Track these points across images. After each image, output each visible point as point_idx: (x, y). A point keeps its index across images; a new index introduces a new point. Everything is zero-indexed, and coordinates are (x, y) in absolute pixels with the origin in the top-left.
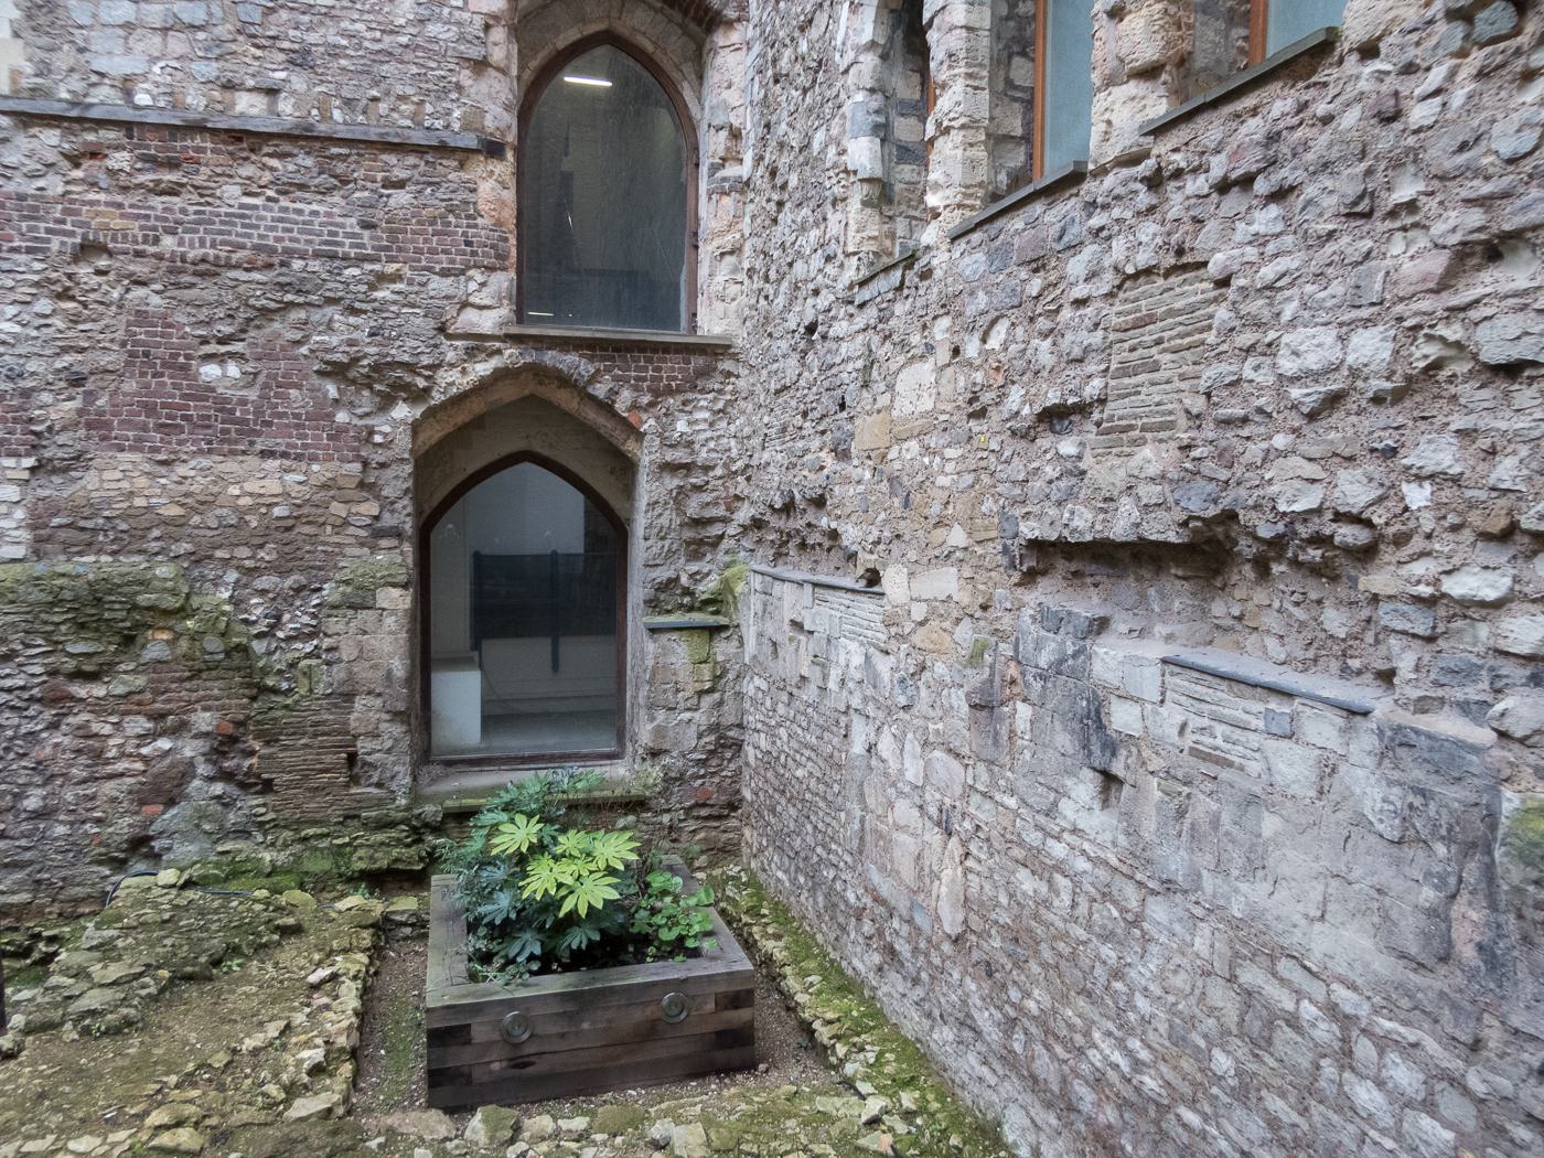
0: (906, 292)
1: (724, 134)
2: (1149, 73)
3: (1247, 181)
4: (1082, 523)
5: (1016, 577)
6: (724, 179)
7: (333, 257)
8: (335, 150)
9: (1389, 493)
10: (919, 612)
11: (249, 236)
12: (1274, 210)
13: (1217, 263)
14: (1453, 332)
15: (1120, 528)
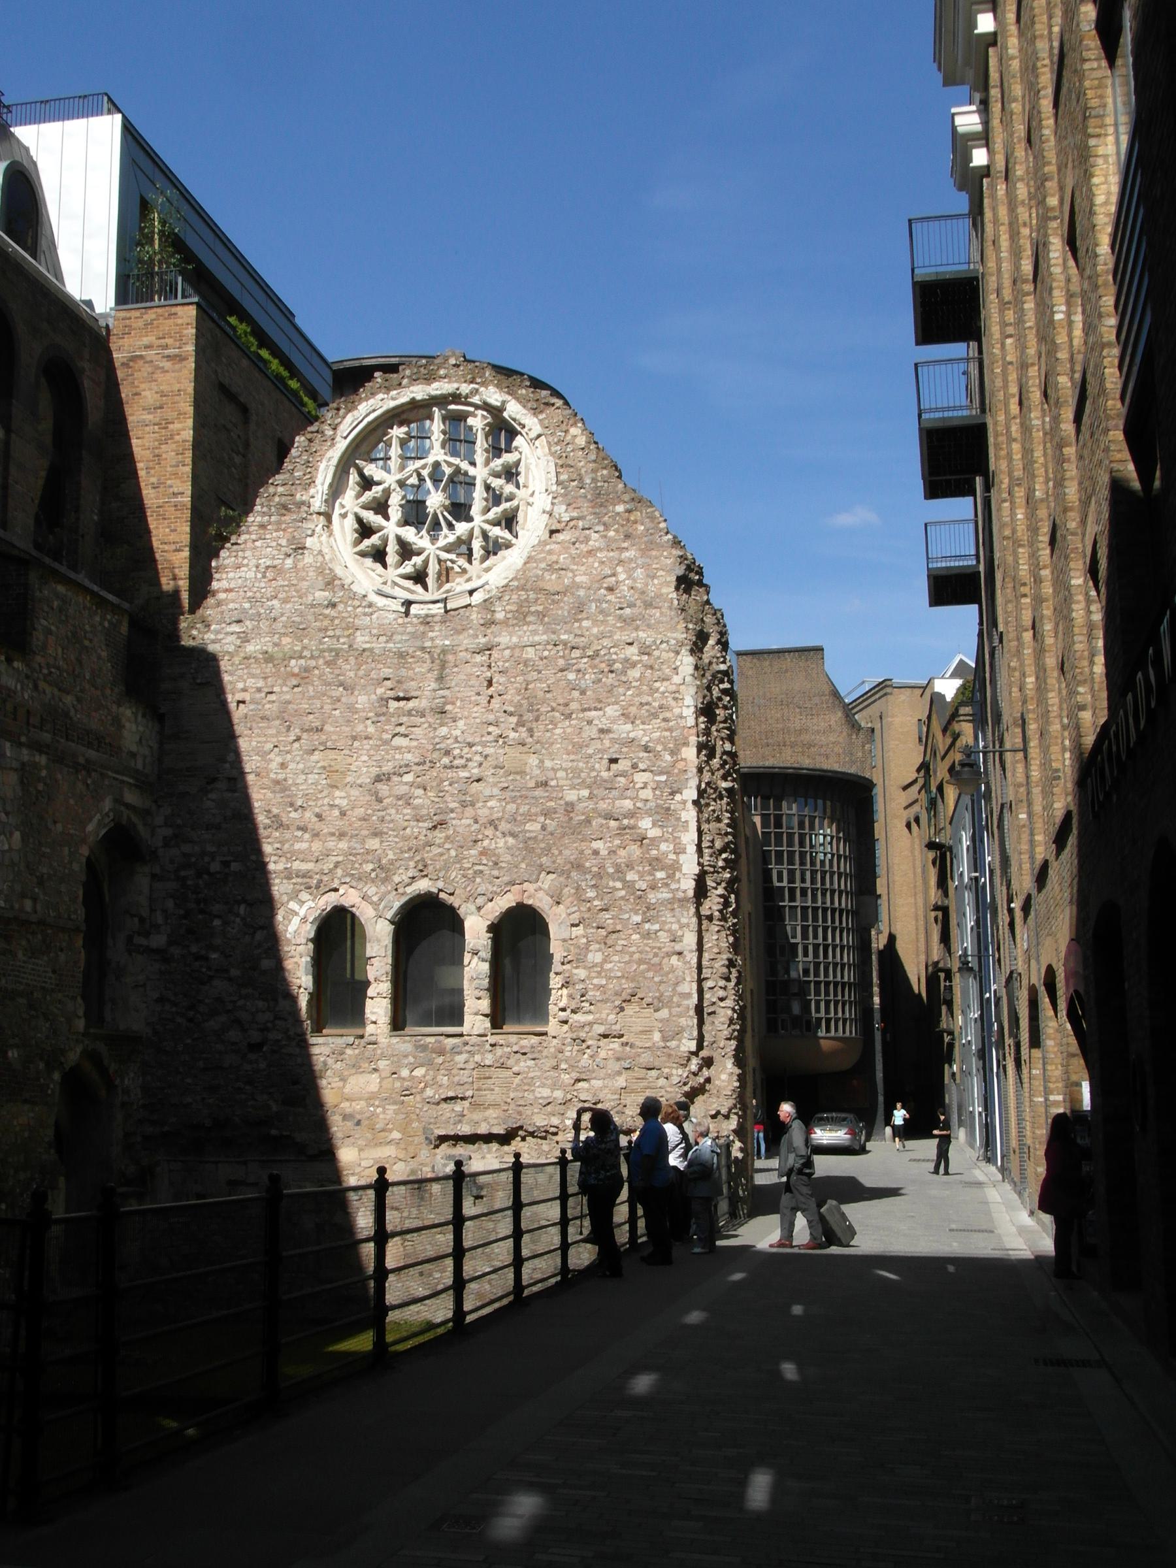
0: (354, 1046)
1: (136, 920)
2: (486, 1016)
3: (524, 1054)
4: (465, 1129)
5: (432, 1146)
6: (141, 946)
7: (43, 988)
8: (49, 931)
9: (563, 1121)
10: (364, 1164)
11: (23, 978)
12: (533, 1062)
13: (516, 1069)
14: (575, 1094)
15: (483, 1129)
